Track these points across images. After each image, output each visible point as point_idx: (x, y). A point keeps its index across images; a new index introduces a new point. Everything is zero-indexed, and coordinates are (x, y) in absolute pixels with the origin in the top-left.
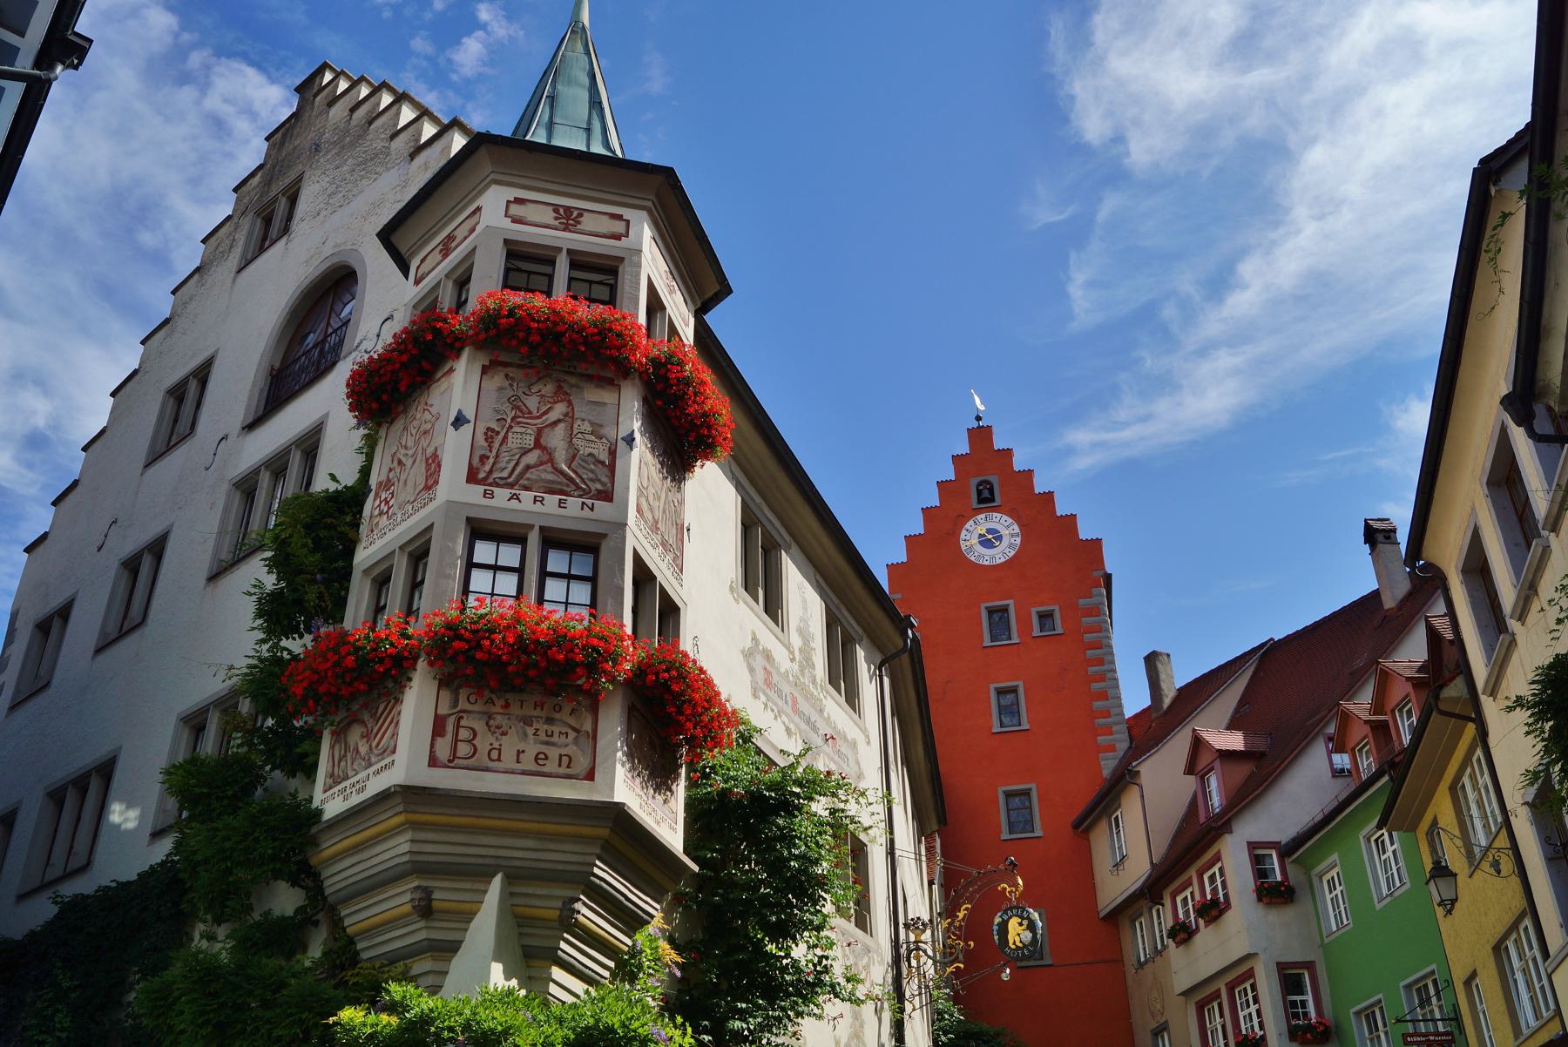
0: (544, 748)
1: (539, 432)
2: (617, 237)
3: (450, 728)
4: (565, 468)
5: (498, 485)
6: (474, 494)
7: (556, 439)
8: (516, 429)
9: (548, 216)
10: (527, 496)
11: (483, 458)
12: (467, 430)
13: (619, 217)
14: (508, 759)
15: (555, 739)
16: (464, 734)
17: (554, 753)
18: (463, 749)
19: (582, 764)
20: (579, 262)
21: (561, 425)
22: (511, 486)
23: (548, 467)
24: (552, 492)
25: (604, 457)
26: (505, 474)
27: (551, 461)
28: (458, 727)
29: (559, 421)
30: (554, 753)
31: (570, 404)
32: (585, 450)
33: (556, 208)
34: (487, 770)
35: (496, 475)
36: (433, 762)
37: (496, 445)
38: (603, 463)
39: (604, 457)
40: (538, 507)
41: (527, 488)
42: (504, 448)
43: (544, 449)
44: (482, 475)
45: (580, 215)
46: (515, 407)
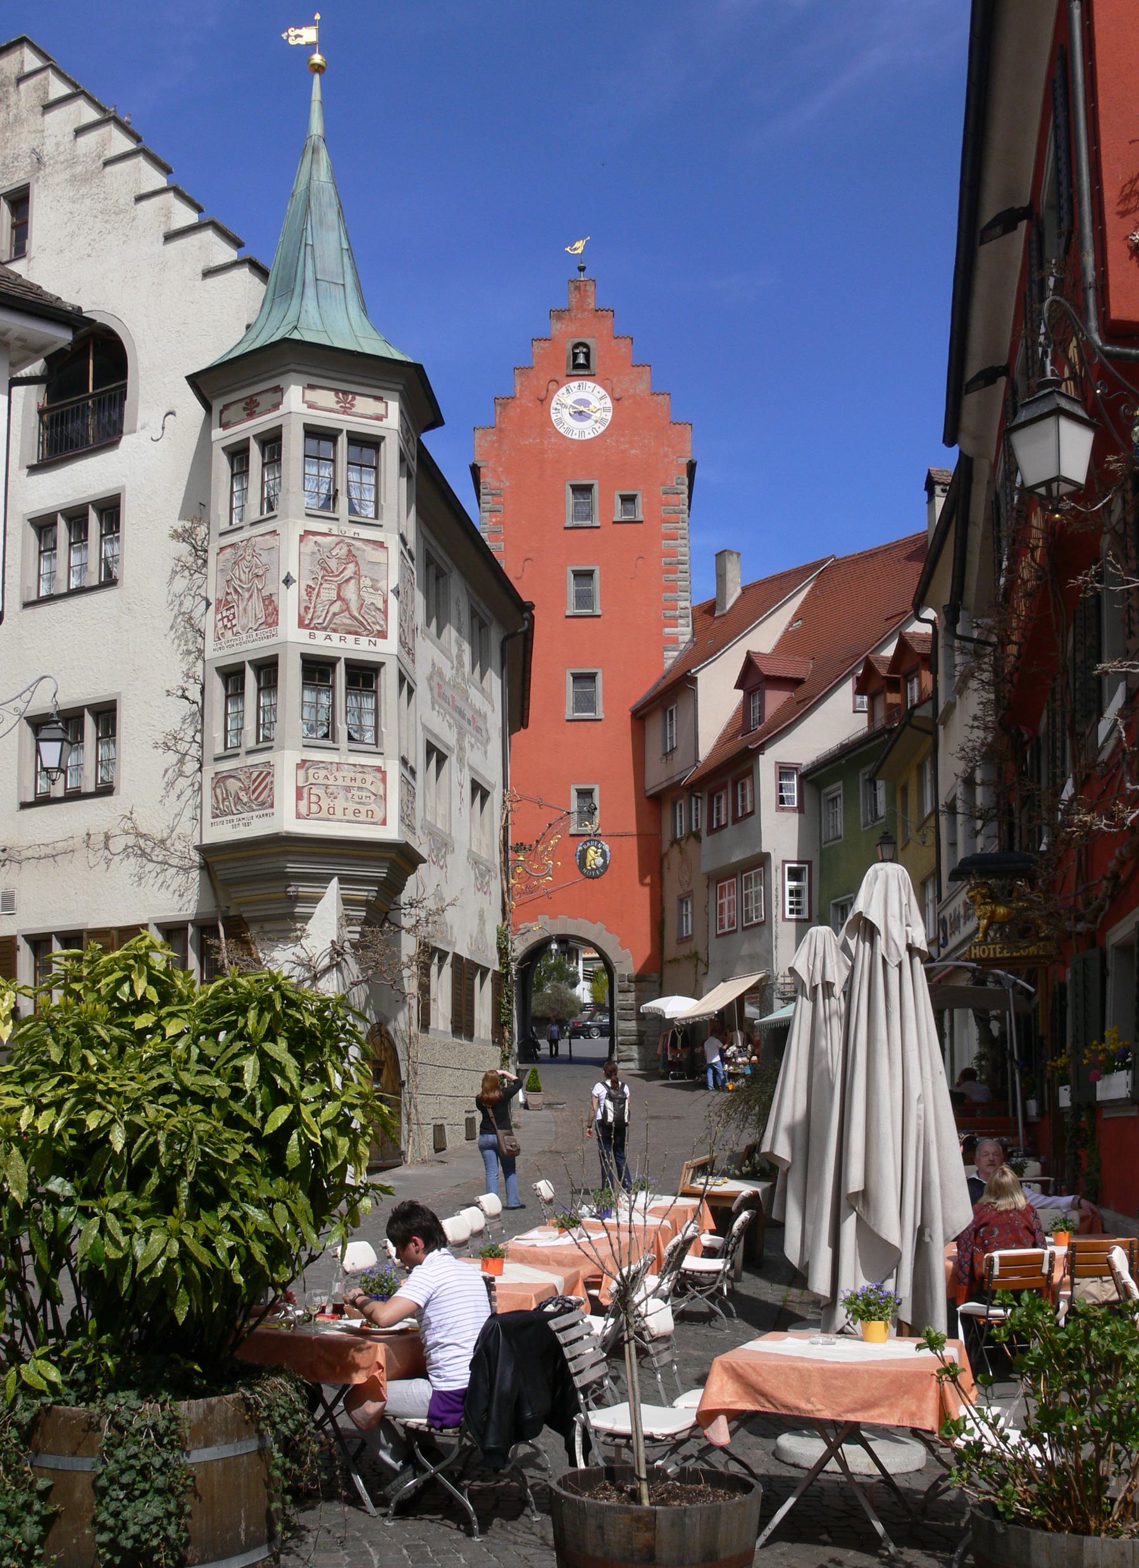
0: (358, 806)
1: (339, 586)
3: (305, 795)
4: (357, 615)
5: (317, 629)
6: (303, 635)
7: (350, 592)
8: (325, 585)
11: (307, 608)
12: (294, 587)
14: (339, 813)
15: (363, 800)
16: (314, 799)
17: (363, 809)
18: (314, 808)
19: (379, 816)
21: (353, 581)
22: (325, 629)
23: (346, 614)
24: (350, 633)
25: (381, 605)
26: (320, 621)
27: (348, 609)
29: (351, 578)
30: (363, 809)
31: (357, 564)
32: (368, 601)
34: (328, 820)
35: (315, 621)
36: (298, 816)
37: (314, 598)
38: (379, 610)
39: (381, 605)
40: (342, 645)
41: (335, 631)
42: (319, 601)
43: (343, 600)
44: (307, 622)
46: (323, 568)
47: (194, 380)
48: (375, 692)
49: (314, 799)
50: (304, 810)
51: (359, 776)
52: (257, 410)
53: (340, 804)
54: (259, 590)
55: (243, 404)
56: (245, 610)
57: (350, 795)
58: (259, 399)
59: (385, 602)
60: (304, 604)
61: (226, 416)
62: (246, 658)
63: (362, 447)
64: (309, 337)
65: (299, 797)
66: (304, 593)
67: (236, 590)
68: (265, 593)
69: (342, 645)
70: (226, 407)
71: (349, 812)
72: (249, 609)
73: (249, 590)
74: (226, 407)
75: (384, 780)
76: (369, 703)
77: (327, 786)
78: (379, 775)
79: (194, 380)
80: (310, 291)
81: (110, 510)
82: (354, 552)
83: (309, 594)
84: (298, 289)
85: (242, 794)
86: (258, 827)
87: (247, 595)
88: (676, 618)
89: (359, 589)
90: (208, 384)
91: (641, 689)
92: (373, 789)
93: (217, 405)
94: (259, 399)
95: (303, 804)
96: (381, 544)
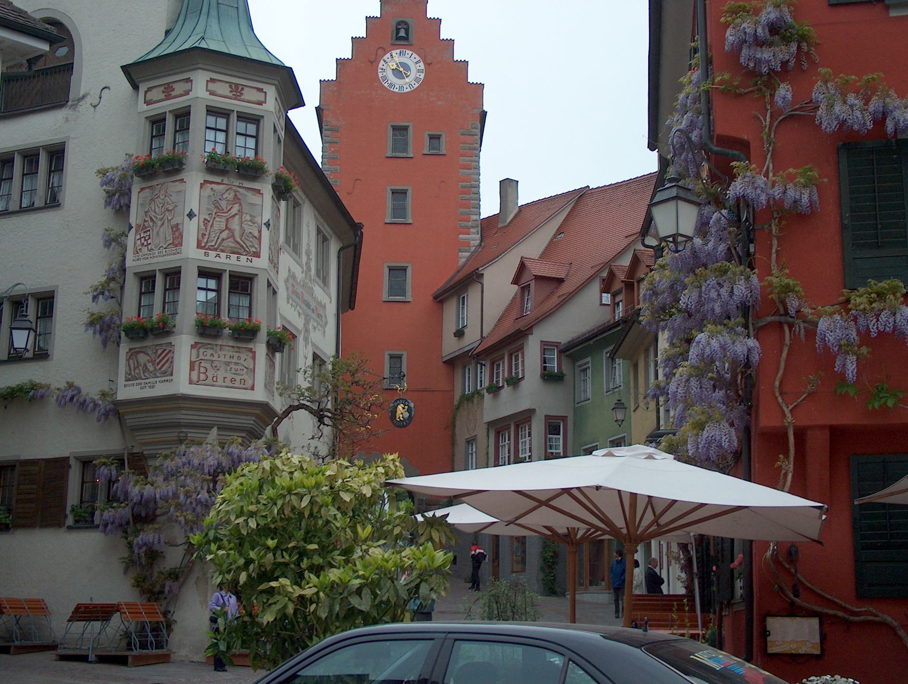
0: (234, 376)
1: (227, 220)
2: (260, 103)
3: (196, 368)
6: (199, 254)
7: (235, 224)
8: (217, 219)
9: (225, 90)
10: (223, 255)
11: (204, 235)
12: (195, 219)
13: (261, 90)
14: (220, 382)
16: (202, 370)
17: (238, 378)
18: (203, 377)
19: (249, 383)
20: (243, 117)
22: (216, 250)
23: (232, 239)
25: (256, 234)
26: (213, 244)
27: (233, 236)
28: (200, 366)
30: (238, 378)
32: (247, 231)
33: (231, 84)
35: (209, 244)
36: (191, 382)
37: (209, 228)
39: (256, 234)
40: (228, 261)
41: (223, 251)
43: (230, 230)
44: (203, 244)
45: (242, 89)
46: (216, 207)
47: (126, 69)
48: (250, 295)
49: (202, 370)
50: (195, 378)
51: (236, 355)
52: (173, 94)
53: (221, 374)
54: (169, 221)
55: (162, 88)
56: (158, 233)
57: (229, 368)
58: (174, 86)
59: (260, 232)
60: (201, 232)
61: (150, 96)
62: (157, 268)
63: (247, 122)
64: (213, 46)
65: (192, 368)
66: (202, 224)
67: (152, 220)
68: (174, 222)
69: (228, 261)
70: (150, 89)
71: (228, 380)
72: (161, 233)
73: (161, 220)
74: (150, 89)
75: (254, 358)
76: (245, 301)
77: (212, 362)
78: (250, 355)
79: (126, 69)
80: (214, 12)
81: (57, 154)
82: (239, 196)
83: (205, 225)
84: (205, 9)
85: (149, 365)
86: (161, 389)
87: (160, 223)
88: (468, 228)
89: (241, 223)
90: (135, 73)
91: (440, 283)
92: (245, 364)
93: (143, 88)
94: (174, 86)
95: (195, 374)
96: (258, 191)
